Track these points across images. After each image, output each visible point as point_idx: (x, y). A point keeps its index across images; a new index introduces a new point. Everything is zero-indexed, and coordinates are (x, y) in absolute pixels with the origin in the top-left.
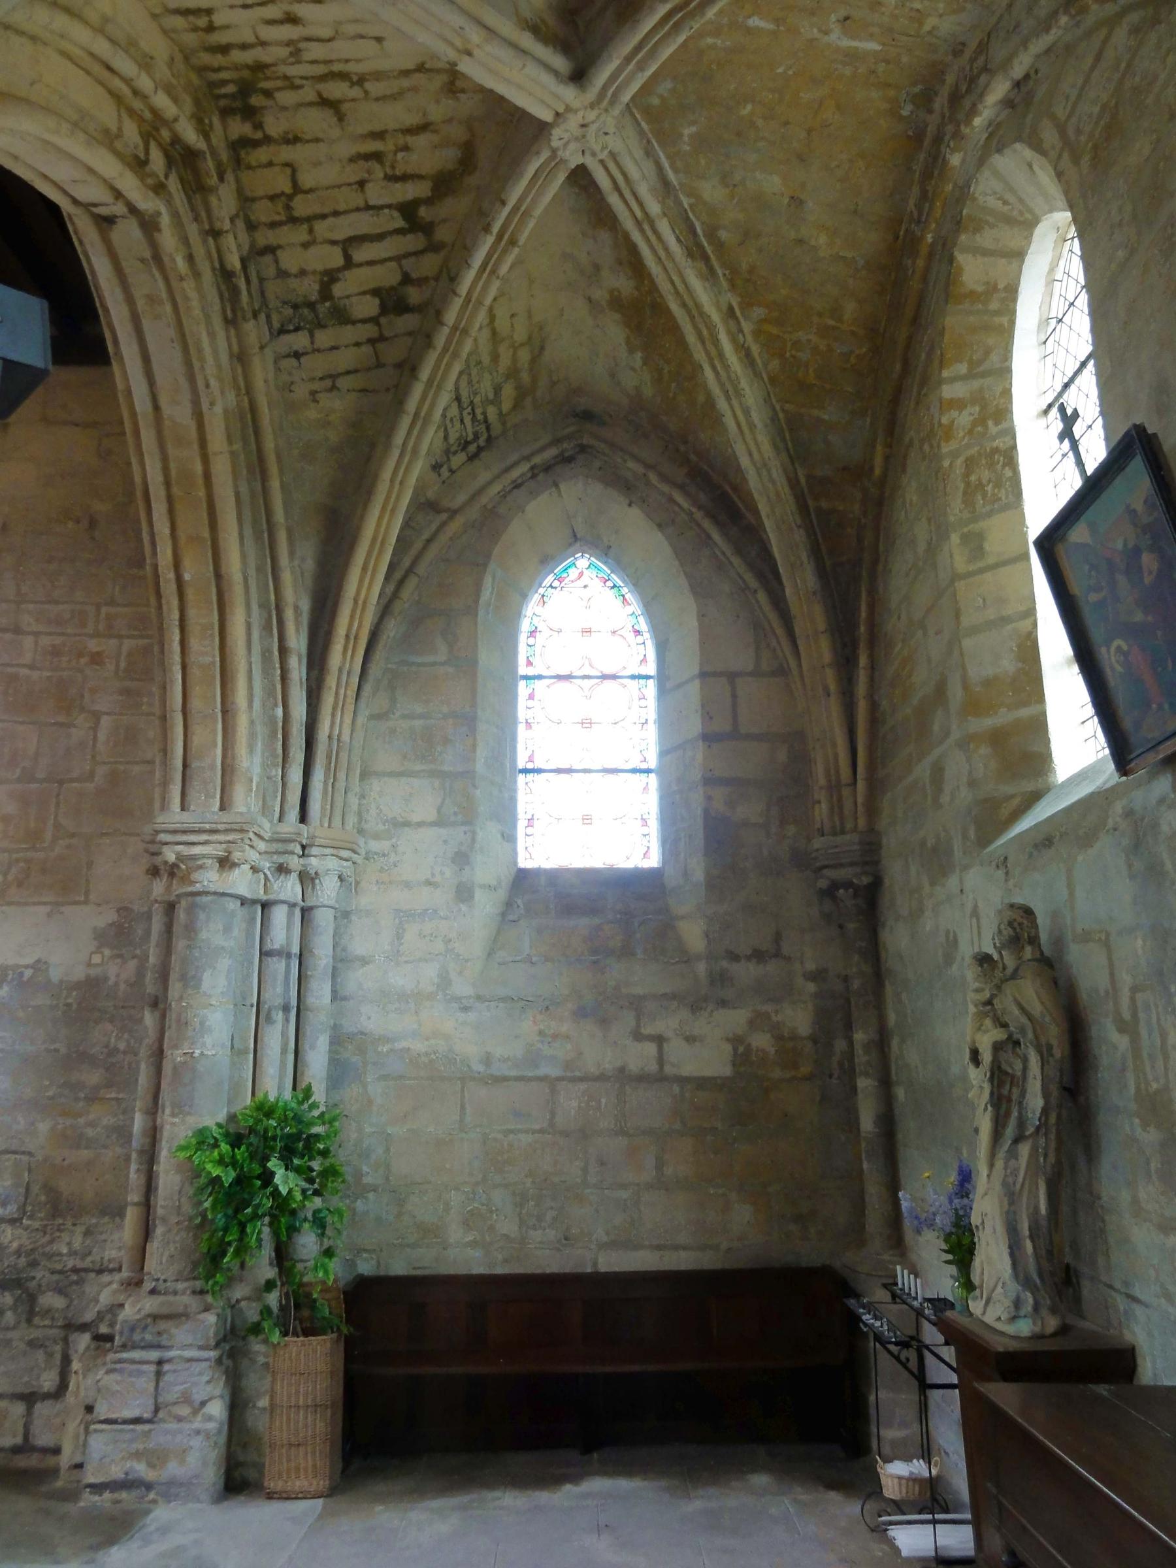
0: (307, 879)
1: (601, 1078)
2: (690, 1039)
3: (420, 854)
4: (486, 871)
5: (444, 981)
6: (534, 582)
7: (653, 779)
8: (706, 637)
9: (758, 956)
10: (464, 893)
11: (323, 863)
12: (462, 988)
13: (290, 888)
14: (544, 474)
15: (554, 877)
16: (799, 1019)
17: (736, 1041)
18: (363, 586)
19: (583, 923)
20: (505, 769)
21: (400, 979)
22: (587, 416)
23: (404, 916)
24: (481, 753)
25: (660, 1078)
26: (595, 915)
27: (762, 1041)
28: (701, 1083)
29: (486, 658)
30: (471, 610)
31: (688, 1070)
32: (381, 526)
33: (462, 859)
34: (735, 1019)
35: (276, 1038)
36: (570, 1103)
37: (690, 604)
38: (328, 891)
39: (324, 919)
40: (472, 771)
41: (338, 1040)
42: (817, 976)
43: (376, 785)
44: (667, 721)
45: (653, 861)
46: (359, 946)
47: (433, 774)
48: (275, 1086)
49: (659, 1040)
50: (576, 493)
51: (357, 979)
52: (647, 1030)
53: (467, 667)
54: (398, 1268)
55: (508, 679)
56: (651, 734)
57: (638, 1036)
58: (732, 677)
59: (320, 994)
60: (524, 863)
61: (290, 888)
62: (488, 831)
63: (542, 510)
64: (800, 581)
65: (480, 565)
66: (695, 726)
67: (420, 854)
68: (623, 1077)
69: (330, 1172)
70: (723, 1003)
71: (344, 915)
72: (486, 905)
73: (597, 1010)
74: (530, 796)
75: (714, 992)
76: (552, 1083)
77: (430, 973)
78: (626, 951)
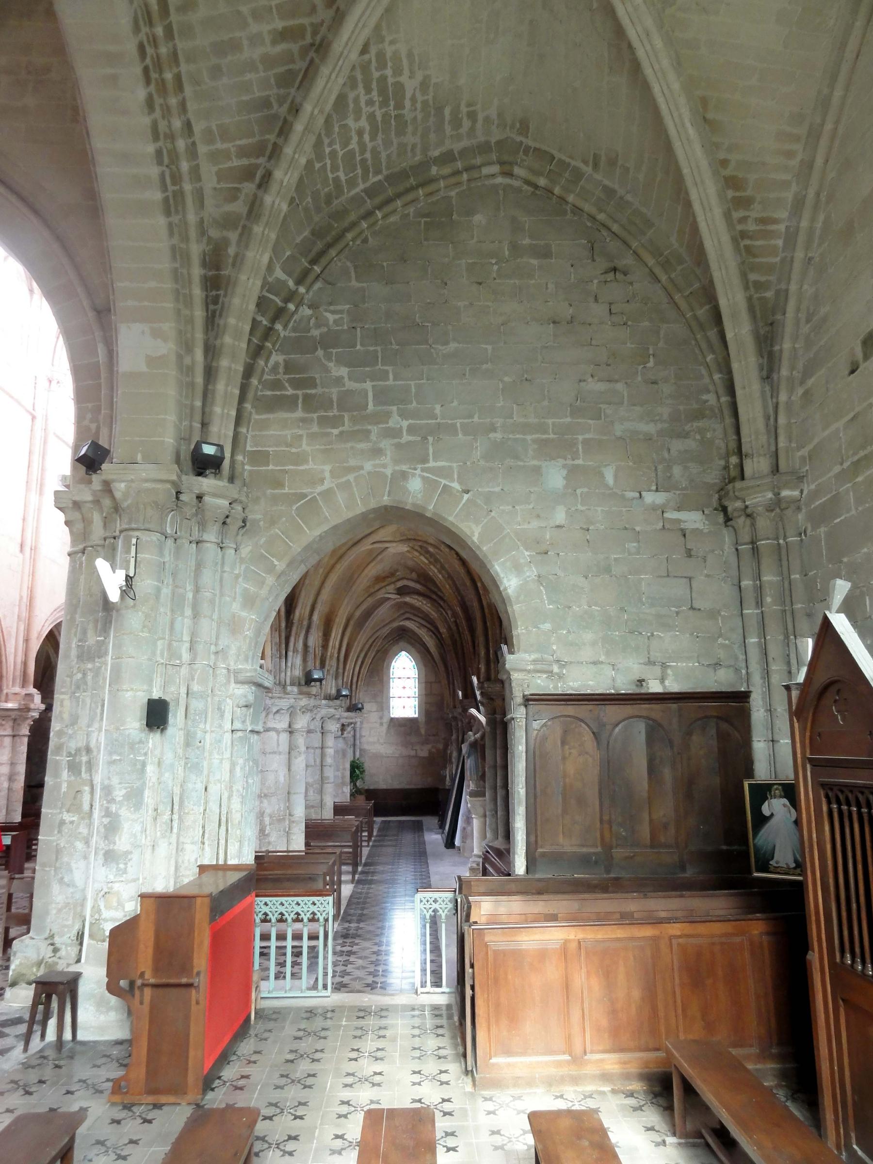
3: (374, 717)
4: (385, 720)
8: (426, 676)
9: (434, 735)
10: (381, 724)
12: (382, 741)
15: (397, 719)
16: (441, 746)
17: (430, 751)
20: (388, 698)
21: (371, 740)
25: (416, 756)
26: (405, 726)
27: (434, 750)
29: (385, 679)
32: (368, 661)
33: (381, 718)
34: (429, 746)
37: (424, 669)
39: (358, 729)
40: (383, 703)
41: (361, 750)
42: (444, 739)
45: (416, 716)
46: (363, 734)
47: (376, 702)
50: (402, 644)
51: (364, 740)
54: (372, 788)
55: (389, 678)
58: (431, 683)
59: (358, 742)
60: (392, 716)
62: (385, 713)
63: (395, 648)
64: (442, 668)
65: (384, 660)
66: (424, 693)
71: (361, 728)
72: (385, 726)
74: (393, 703)
75: (426, 742)
77: (375, 739)
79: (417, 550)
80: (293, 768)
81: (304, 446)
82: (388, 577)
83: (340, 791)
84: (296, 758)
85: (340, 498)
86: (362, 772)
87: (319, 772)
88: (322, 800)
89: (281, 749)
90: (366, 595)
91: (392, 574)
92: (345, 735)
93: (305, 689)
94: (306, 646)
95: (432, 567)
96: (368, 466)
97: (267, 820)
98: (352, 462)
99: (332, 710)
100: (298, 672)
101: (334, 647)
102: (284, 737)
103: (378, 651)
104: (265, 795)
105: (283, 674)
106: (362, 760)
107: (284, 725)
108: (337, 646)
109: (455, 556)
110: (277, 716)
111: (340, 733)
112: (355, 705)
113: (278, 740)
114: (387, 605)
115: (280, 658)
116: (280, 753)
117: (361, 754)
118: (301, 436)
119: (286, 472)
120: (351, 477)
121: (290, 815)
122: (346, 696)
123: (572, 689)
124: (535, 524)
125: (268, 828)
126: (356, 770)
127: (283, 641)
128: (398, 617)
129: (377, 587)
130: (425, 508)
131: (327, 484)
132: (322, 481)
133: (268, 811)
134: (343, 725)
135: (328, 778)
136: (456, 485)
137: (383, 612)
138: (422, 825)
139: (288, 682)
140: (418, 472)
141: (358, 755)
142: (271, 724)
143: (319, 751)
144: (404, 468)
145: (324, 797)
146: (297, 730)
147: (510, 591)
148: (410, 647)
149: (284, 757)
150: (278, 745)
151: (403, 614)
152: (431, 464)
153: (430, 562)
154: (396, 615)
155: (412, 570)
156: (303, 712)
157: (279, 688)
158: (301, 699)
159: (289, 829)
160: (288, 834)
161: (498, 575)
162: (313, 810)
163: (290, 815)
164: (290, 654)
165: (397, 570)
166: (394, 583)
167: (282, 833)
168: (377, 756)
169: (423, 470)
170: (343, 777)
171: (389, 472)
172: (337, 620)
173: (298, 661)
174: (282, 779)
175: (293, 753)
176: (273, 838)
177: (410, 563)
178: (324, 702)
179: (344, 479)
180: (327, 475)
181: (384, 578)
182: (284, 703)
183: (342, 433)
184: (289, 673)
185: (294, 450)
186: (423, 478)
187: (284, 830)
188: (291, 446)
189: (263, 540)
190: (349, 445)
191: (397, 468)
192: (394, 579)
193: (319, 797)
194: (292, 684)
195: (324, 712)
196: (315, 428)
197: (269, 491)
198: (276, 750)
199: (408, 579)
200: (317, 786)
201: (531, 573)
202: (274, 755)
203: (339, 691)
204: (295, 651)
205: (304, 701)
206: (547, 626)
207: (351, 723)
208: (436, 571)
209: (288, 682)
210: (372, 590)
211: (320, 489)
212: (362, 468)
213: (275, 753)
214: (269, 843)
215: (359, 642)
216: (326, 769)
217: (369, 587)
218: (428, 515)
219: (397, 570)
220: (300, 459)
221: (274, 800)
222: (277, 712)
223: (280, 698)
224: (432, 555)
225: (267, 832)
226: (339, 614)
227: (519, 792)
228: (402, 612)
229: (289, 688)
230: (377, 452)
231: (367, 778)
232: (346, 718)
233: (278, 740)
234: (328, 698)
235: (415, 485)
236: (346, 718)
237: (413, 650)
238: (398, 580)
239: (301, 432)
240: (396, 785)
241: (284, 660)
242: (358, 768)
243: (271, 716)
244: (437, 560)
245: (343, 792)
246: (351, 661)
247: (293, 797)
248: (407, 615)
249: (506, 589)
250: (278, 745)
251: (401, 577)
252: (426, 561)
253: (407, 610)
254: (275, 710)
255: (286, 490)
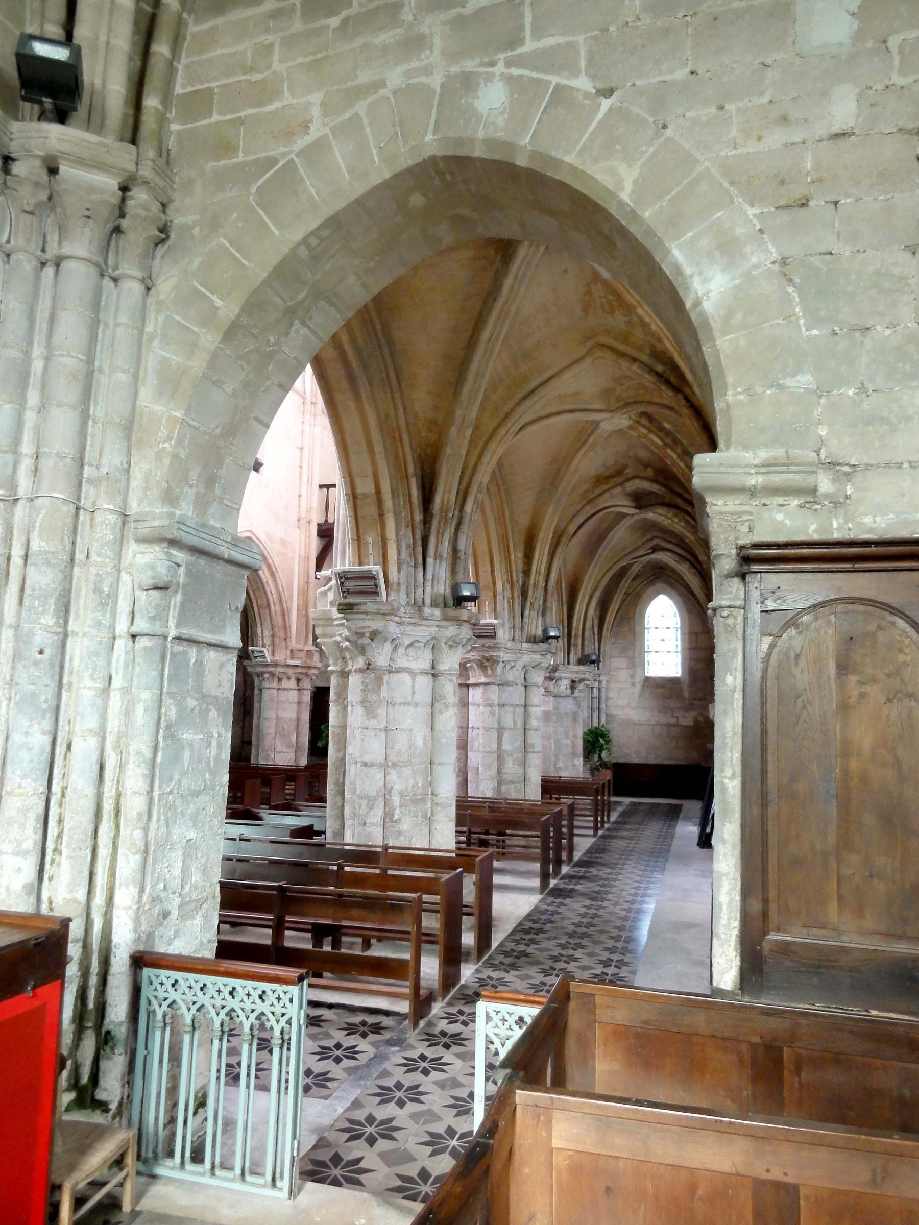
0: (600, 682)
1: (665, 725)
2: (684, 717)
3: (623, 675)
4: (639, 679)
5: (629, 703)
6: (649, 604)
7: (679, 654)
9: (700, 699)
10: (633, 684)
11: (603, 678)
12: (633, 705)
13: (596, 684)
14: (652, 582)
15: (654, 679)
18: (610, 617)
19: (661, 690)
20: (642, 652)
21: (620, 703)
22: (661, 568)
23: (621, 689)
24: (637, 651)
25: (677, 725)
26: (665, 688)
27: (700, 718)
28: (686, 727)
29: (638, 628)
30: (634, 617)
31: (684, 724)
32: (614, 607)
33: (633, 676)
34: (695, 713)
35: (595, 715)
36: (657, 730)
37: (686, 614)
38: (604, 684)
39: (603, 690)
41: (607, 715)
43: (613, 660)
44: (683, 640)
46: (610, 695)
47: (627, 657)
48: (595, 724)
49: (677, 717)
50: (659, 585)
51: (610, 703)
52: (675, 714)
53: (633, 631)
54: (621, 761)
55: (644, 628)
56: (679, 643)
57: (672, 716)
59: (603, 706)
60: (647, 675)
61: (596, 684)
62: (638, 670)
63: (651, 590)
65: (636, 605)
66: (687, 645)
67: (623, 675)
68: (669, 725)
69: (610, 740)
70: (692, 710)
71: (607, 689)
72: (638, 687)
73: (664, 710)
74: (648, 657)
75: (689, 707)
76: (653, 726)
77: (626, 702)
78: (670, 697)
79: (644, 426)
80: (438, 727)
81: (276, 65)
82: (613, 476)
83: (570, 764)
84: (441, 712)
85: (339, 155)
86: (608, 742)
87: (520, 738)
88: (525, 774)
89: (418, 698)
90: (584, 503)
91: (619, 473)
92: (576, 694)
93: (452, 612)
94: (455, 550)
95: (669, 451)
96: (395, 77)
97: (396, 800)
98: (364, 77)
99: (537, 657)
100: (443, 588)
101: (538, 572)
102: (424, 682)
103: (627, 594)
104: (394, 765)
105: (420, 590)
106: (610, 727)
107: (427, 665)
108: (543, 571)
109: (684, 402)
110: (411, 651)
111: (569, 691)
112: (588, 656)
113: (413, 686)
114: (626, 523)
115: (415, 567)
116: (416, 705)
117: (607, 720)
118: (271, 46)
119: (241, 122)
120: (361, 108)
121: (433, 794)
122: (556, 638)
123: (871, 531)
124: (776, 138)
125: (397, 811)
126: (595, 741)
127: (419, 542)
128: (644, 543)
129: (598, 491)
130: (510, 146)
131: (315, 132)
132: (305, 127)
133: (398, 787)
134: (573, 682)
135: (533, 746)
136: (583, 83)
137: (621, 535)
138: (680, 812)
139: (428, 601)
140: (500, 68)
141: (603, 721)
142: (402, 662)
143: (522, 710)
144: (469, 65)
145: (528, 770)
146: (442, 673)
147: (707, 306)
148: (669, 589)
149: (423, 712)
150: (414, 693)
151: (651, 539)
152: (529, 46)
153: (666, 444)
154: (640, 542)
155: (647, 466)
156: (451, 647)
157: (409, 610)
158: (446, 628)
159: (432, 814)
160: (430, 820)
161: (678, 271)
162: (512, 786)
163: (433, 794)
164: (430, 561)
165: (625, 467)
166: (621, 484)
167: (420, 819)
168: (627, 723)
169: (509, 64)
170: (574, 746)
171: (436, 81)
172: (541, 535)
173: (443, 571)
174: (420, 742)
175: (437, 706)
176: (405, 826)
177: (643, 454)
178: (525, 645)
179: (347, 115)
180: (316, 112)
181: (608, 478)
182: (422, 632)
183: (345, 22)
184: (428, 590)
185: (257, 77)
186: (510, 80)
187: (425, 816)
188: (252, 70)
189: (197, 261)
190: (359, 42)
191: (454, 69)
192: (620, 479)
193: (521, 770)
194: (434, 605)
195: (526, 658)
196: (297, 25)
197: (211, 164)
198: (410, 699)
199: (641, 478)
200: (519, 756)
201: (761, 257)
202: (406, 708)
203: (545, 631)
204: (438, 557)
205: (451, 631)
206: (805, 380)
207: (583, 680)
208: (675, 457)
209: (428, 601)
210: (592, 496)
211: (301, 142)
212: (382, 84)
213: (407, 704)
214: (400, 833)
215: (591, 577)
216: (531, 734)
217: (587, 491)
218: (522, 161)
219: (625, 467)
220: (266, 92)
221: (407, 771)
222: (411, 645)
223: (414, 624)
224: (668, 433)
225: (396, 817)
226: (544, 527)
227: (724, 788)
228: (649, 537)
229: (427, 611)
230: (415, 43)
231: (614, 749)
232: (577, 673)
233: (413, 686)
234: (533, 640)
235: (492, 98)
236: (577, 673)
237: (674, 592)
238: (628, 480)
239: (270, 38)
240: (652, 760)
241: (421, 569)
242: (603, 735)
243: (401, 651)
244: (676, 441)
245: (574, 765)
246: (582, 601)
247: (437, 769)
248: (656, 541)
249: (698, 303)
250: (414, 693)
251: (630, 475)
252: (660, 443)
253: (655, 534)
254: (407, 642)
255: (241, 158)
